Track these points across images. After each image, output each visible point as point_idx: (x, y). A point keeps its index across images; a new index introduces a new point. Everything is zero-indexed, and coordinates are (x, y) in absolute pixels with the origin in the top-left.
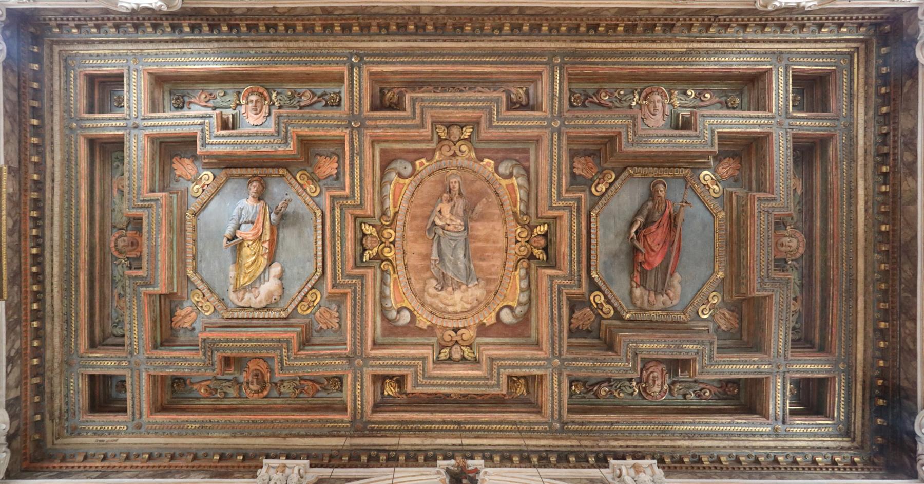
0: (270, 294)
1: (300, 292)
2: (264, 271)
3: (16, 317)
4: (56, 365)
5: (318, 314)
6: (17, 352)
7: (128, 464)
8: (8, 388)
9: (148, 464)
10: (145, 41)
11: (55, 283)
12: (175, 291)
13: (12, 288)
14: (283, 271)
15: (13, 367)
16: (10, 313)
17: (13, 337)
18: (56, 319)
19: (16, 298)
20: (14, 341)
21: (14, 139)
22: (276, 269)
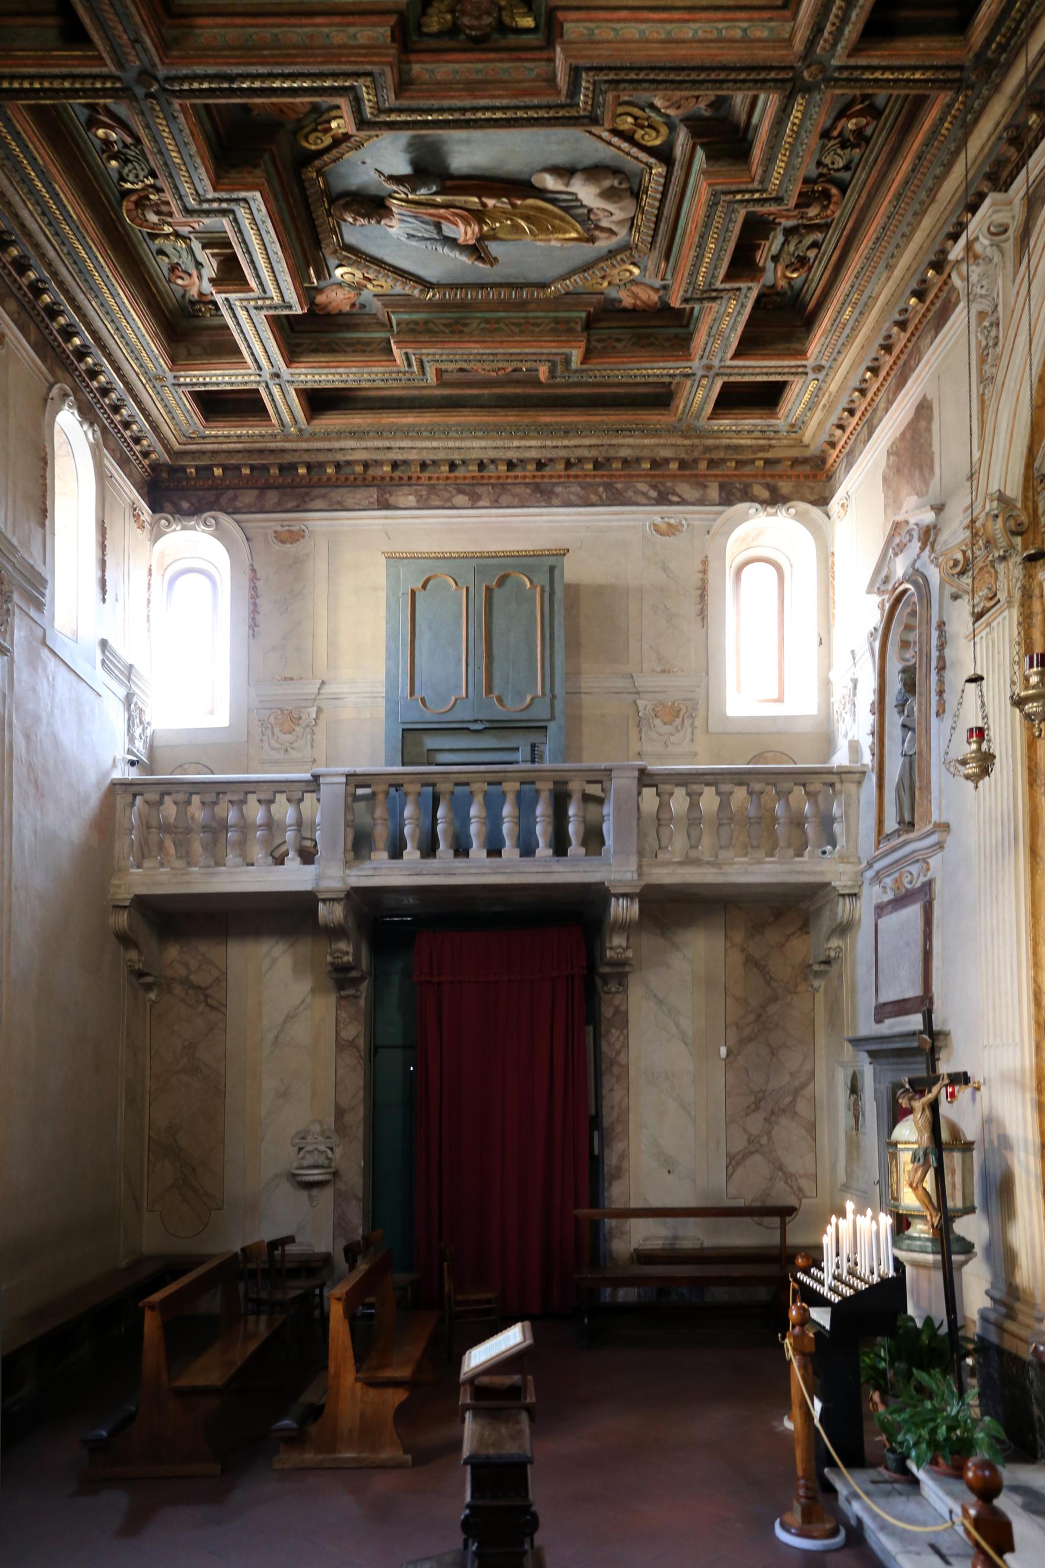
0: (608, 194)
1: (609, 143)
2: (553, 201)
3: (601, 489)
4: (686, 442)
5: (671, 112)
6: (654, 487)
7: (870, 395)
8: (701, 502)
9: (881, 378)
10: (122, 377)
11: (554, 443)
12: (584, 315)
13: (557, 495)
14: (556, 170)
15: (675, 493)
16: (593, 498)
17: (630, 493)
18: (614, 441)
19: (573, 489)
20: (637, 492)
21: (336, 495)
22: (551, 183)
